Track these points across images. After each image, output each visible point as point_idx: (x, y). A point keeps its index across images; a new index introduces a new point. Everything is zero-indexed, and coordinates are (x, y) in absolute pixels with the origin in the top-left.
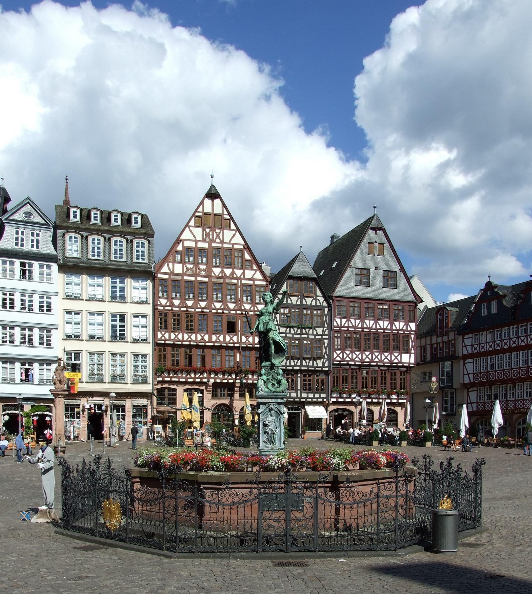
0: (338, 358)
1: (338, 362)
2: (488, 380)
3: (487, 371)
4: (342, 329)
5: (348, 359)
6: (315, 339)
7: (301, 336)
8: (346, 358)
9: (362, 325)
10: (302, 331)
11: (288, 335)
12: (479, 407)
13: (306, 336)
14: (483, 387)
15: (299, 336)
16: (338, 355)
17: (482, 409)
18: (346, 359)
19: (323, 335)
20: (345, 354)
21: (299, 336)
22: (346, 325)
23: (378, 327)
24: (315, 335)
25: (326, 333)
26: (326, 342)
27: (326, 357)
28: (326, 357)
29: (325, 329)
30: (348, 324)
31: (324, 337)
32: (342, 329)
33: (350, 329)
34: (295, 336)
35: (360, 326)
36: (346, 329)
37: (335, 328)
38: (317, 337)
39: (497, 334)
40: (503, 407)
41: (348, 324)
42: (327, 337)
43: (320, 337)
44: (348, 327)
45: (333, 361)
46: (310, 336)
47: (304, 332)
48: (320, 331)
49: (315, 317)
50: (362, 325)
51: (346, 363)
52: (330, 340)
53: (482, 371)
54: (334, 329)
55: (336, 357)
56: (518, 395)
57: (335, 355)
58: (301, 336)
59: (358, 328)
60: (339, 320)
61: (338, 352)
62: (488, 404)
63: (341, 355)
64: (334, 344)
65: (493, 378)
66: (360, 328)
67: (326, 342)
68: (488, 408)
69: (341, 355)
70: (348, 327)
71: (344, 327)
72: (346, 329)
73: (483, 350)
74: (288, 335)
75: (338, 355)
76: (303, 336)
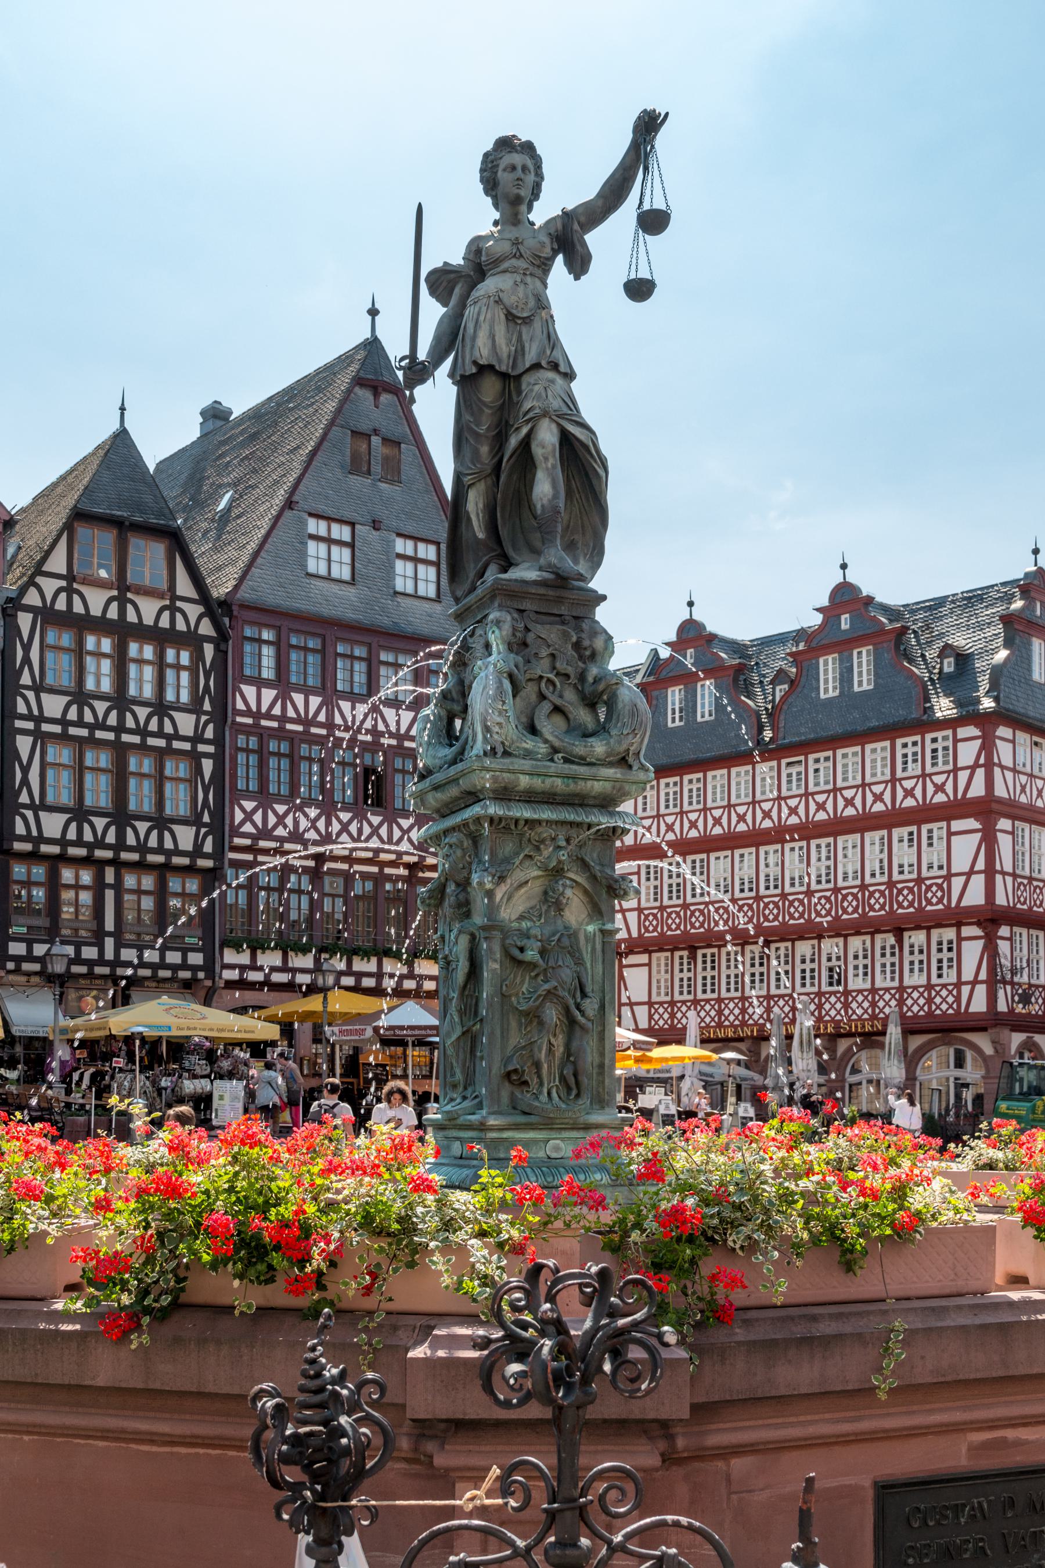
0: (248, 828)
1: (248, 842)
2: (686, 932)
3: (681, 902)
4: (264, 723)
5: (280, 832)
6: (169, 751)
7: (118, 737)
8: (275, 827)
9: (330, 716)
10: (121, 719)
11: (73, 731)
12: (656, 1017)
13: (136, 739)
14: (668, 954)
15: (110, 736)
16: (248, 817)
17: (713, 1020)
18: (276, 833)
19: (197, 738)
20: (270, 813)
21: (110, 736)
22: (277, 711)
23: (381, 727)
24: (169, 738)
25: (209, 733)
26: (207, 765)
27: (206, 818)
28: (206, 818)
29: (204, 718)
30: (284, 708)
31: (202, 748)
32: (264, 723)
33: (289, 726)
34: (99, 734)
35: (322, 718)
36: (275, 724)
37: (239, 719)
38: (177, 745)
39: (789, 775)
40: (708, 1020)
41: (284, 708)
42: (210, 749)
43: (187, 746)
44: (283, 719)
45: (231, 837)
46: (151, 741)
47: (130, 723)
48: (186, 723)
49: (170, 675)
50: (330, 716)
51: (273, 845)
52: (218, 758)
53: (666, 902)
54: (234, 722)
55: (242, 823)
57: (239, 816)
58: (118, 737)
59: (312, 723)
60: (254, 689)
61: (249, 805)
62: (661, 1010)
63: (258, 817)
64: (234, 776)
65: (702, 925)
66: (320, 725)
67: (207, 765)
68: (859, 1012)
69: (258, 817)
70: (283, 719)
71: (269, 716)
72: (275, 724)
73: (694, 834)
74: (73, 731)
75: (248, 817)
76: (126, 738)
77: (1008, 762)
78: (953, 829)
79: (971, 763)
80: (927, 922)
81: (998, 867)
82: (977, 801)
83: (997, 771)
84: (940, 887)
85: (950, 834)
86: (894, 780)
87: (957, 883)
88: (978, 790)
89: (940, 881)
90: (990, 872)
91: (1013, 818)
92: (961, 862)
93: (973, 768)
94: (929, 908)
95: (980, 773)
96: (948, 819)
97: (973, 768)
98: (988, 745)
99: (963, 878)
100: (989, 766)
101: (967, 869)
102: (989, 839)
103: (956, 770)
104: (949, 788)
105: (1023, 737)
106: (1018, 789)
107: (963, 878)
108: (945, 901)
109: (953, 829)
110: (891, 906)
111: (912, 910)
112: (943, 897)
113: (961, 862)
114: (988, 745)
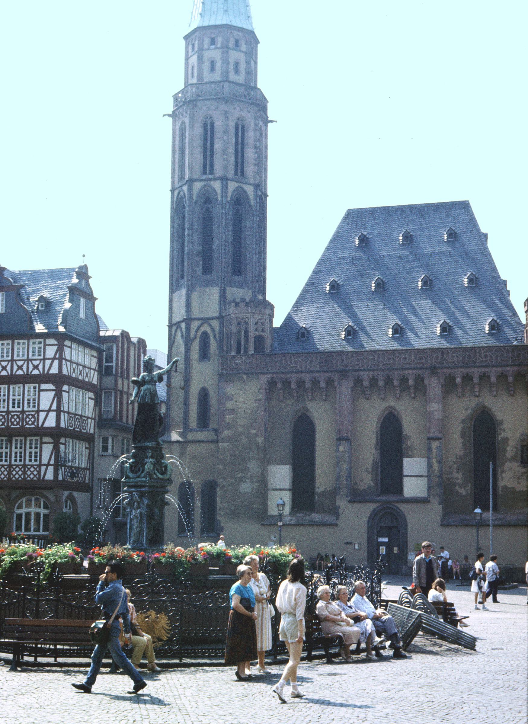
56: (16, 457)
77: (68, 357)
78: (41, 388)
79: (52, 356)
80: (24, 433)
81: (62, 409)
82: (54, 375)
83: (64, 361)
84: (33, 416)
85: (40, 390)
86: (12, 360)
87: (42, 415)
88: (54, 370)
89: (33, 413)
90: (59, 411)
91: (69, 384)
92: (45, 404)
93: (53, 359)
94: (27, 426)
95: (56, 362)
96: (40, 383)
97: (53, 359)
98: (60, 349)
99: (46, 413)
100: (61, 359)
101: (47, 408)
102: (58, 395)
103: (44, 359)
104: (41, 367)
105: (74, 346)
106: (72, 371)
107: (46, 413)
108: (36, 424)
109: (41, 388)
110: (8, 423)
111: (18, 426)
112: (35, 421)
113: (45, 404)
114: (60, 349)
